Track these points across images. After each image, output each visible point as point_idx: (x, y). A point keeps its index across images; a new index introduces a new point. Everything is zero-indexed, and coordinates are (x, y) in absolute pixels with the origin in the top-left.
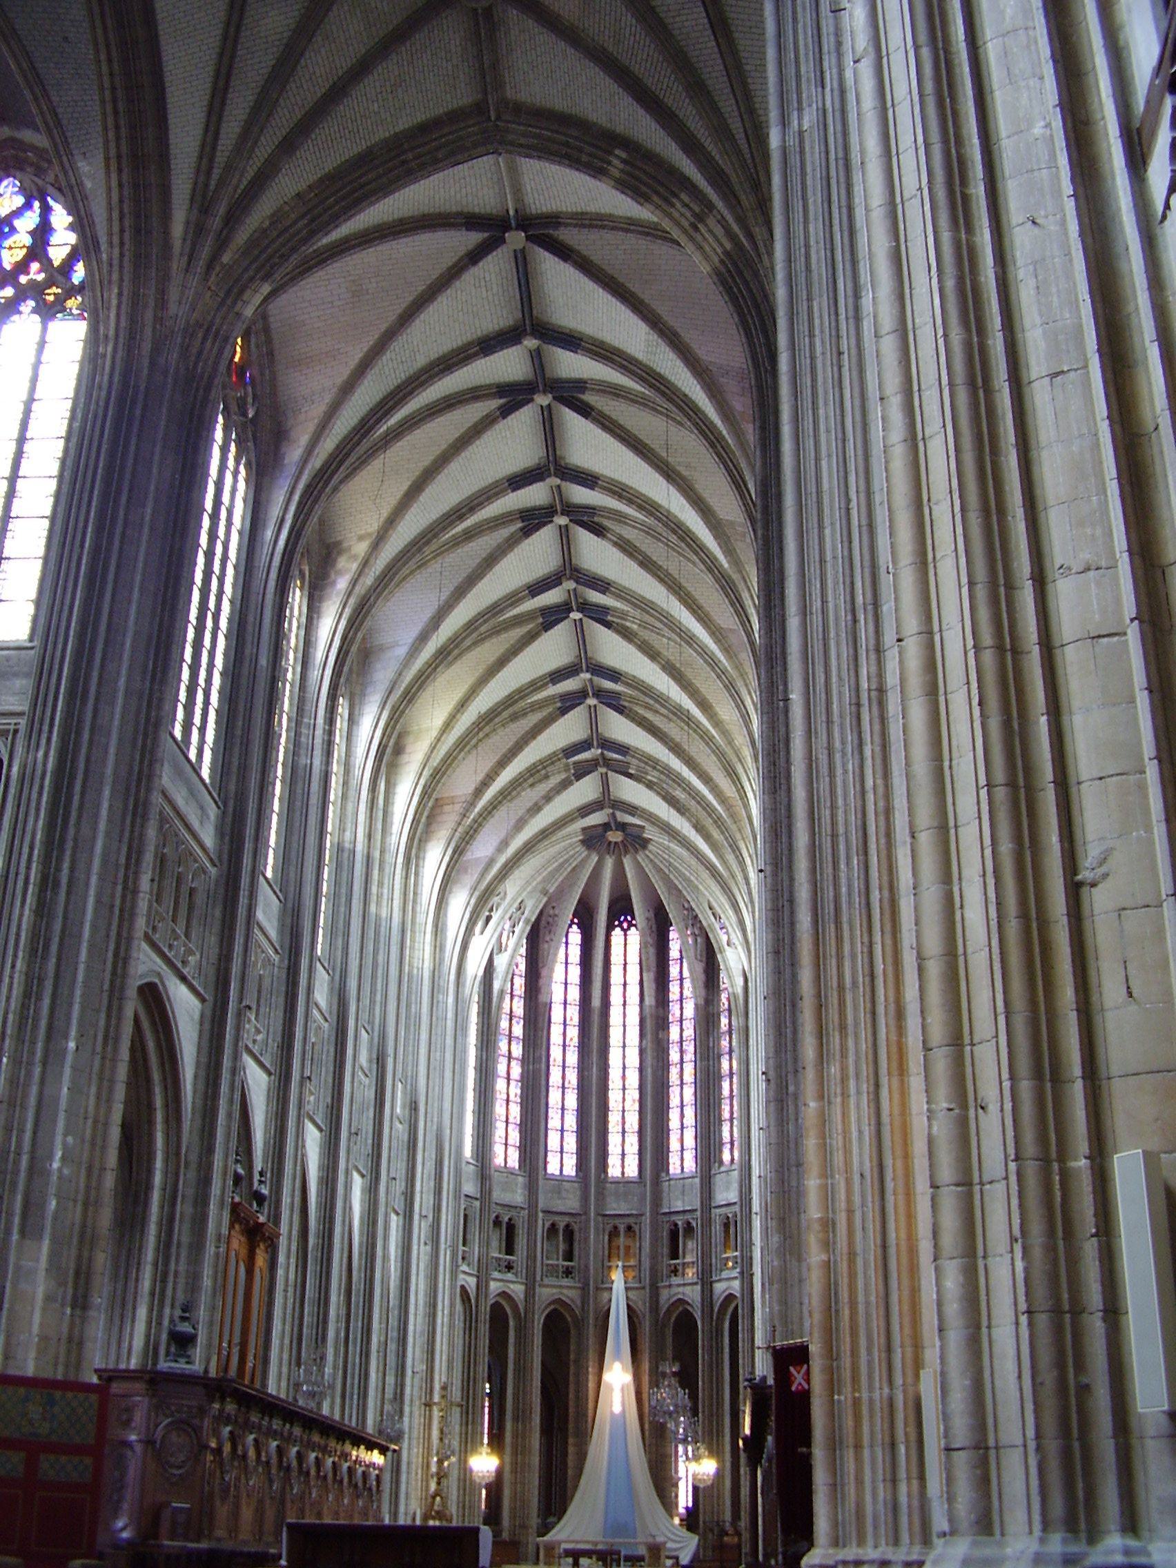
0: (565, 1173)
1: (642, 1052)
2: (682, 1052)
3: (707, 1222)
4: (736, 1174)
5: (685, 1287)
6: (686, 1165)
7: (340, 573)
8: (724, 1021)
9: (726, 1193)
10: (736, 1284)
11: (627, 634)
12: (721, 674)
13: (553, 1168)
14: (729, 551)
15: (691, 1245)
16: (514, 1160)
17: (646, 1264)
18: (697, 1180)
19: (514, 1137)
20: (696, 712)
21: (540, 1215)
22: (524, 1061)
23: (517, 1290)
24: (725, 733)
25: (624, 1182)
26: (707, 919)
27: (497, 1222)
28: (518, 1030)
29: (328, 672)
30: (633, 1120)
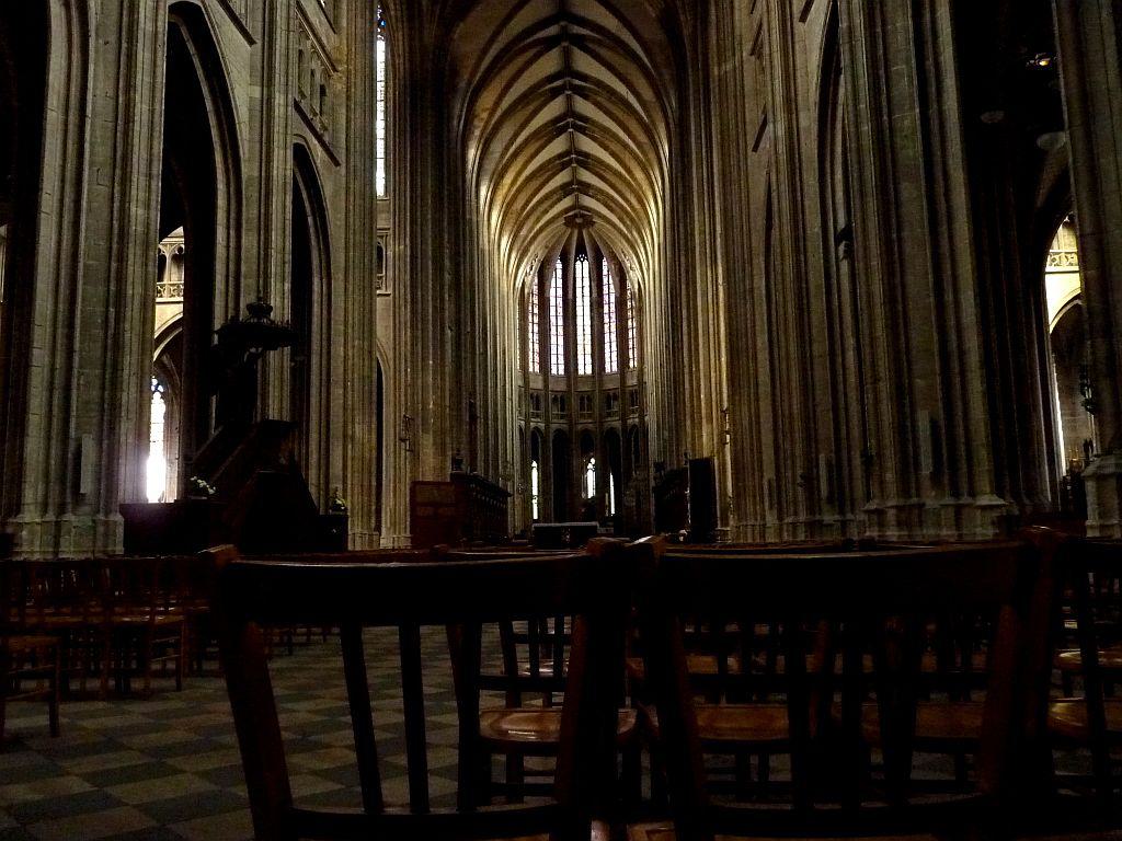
1: (592, 318)
3: (623, 392)
4: (636, 373)
5: (615, 423)
7: (476, 127)
8: (629, 304)
9: (632, 381)
10: (637, 420)
11: (594, 139)
12: (640, 163)
13: (554, 371)
14: (649, 116)
15: (616, 403)
17: (597, 411)
19: (537, 359)
20: (623, 172)
23: (542, 426)
24: (639, 185)
25: (585, 376)
26: (621, 257)
27: (532, 397)
28: (536, 311)
29: (474, 175)
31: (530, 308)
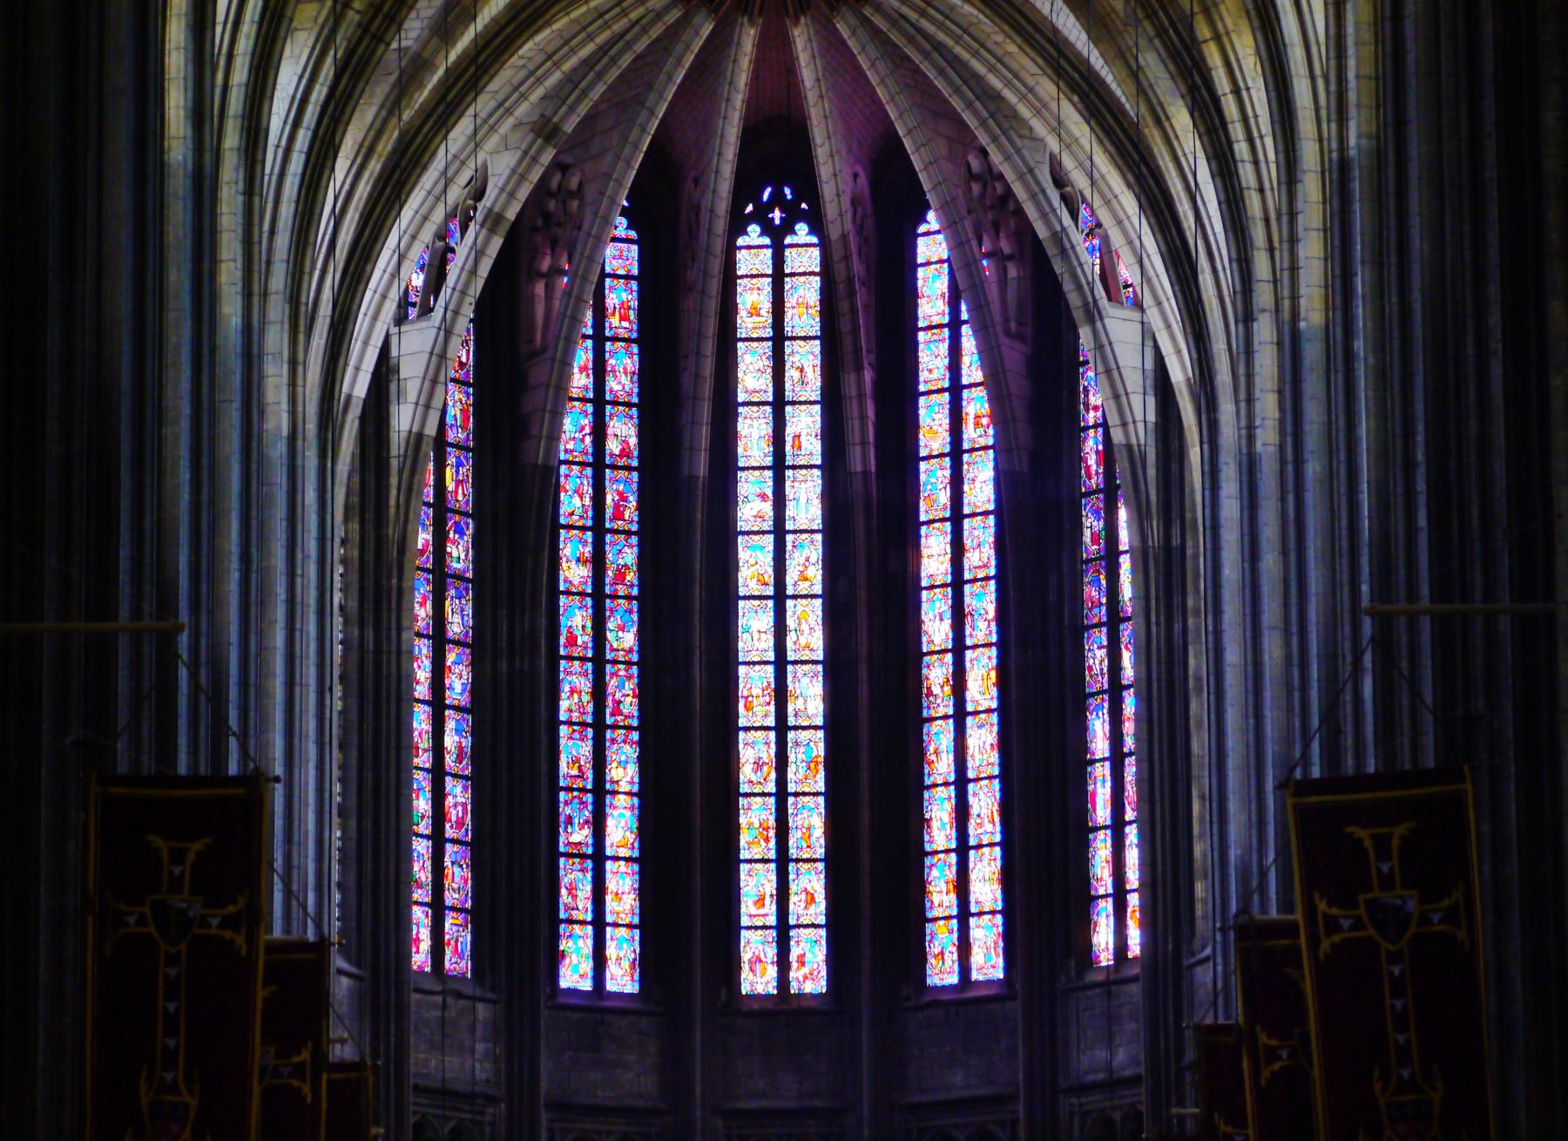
0: (611, 986)
2: (959, 615)
6: (977, 957)
8: (1092, 524)
13: (575, 974)
16: (458, 962)
18: (1015, 1008)
19: (458, 877)
21: (544, 1116)
22: (480, 647)
28: (459, 554)
30: (810, 823)
31: (424, 537)
